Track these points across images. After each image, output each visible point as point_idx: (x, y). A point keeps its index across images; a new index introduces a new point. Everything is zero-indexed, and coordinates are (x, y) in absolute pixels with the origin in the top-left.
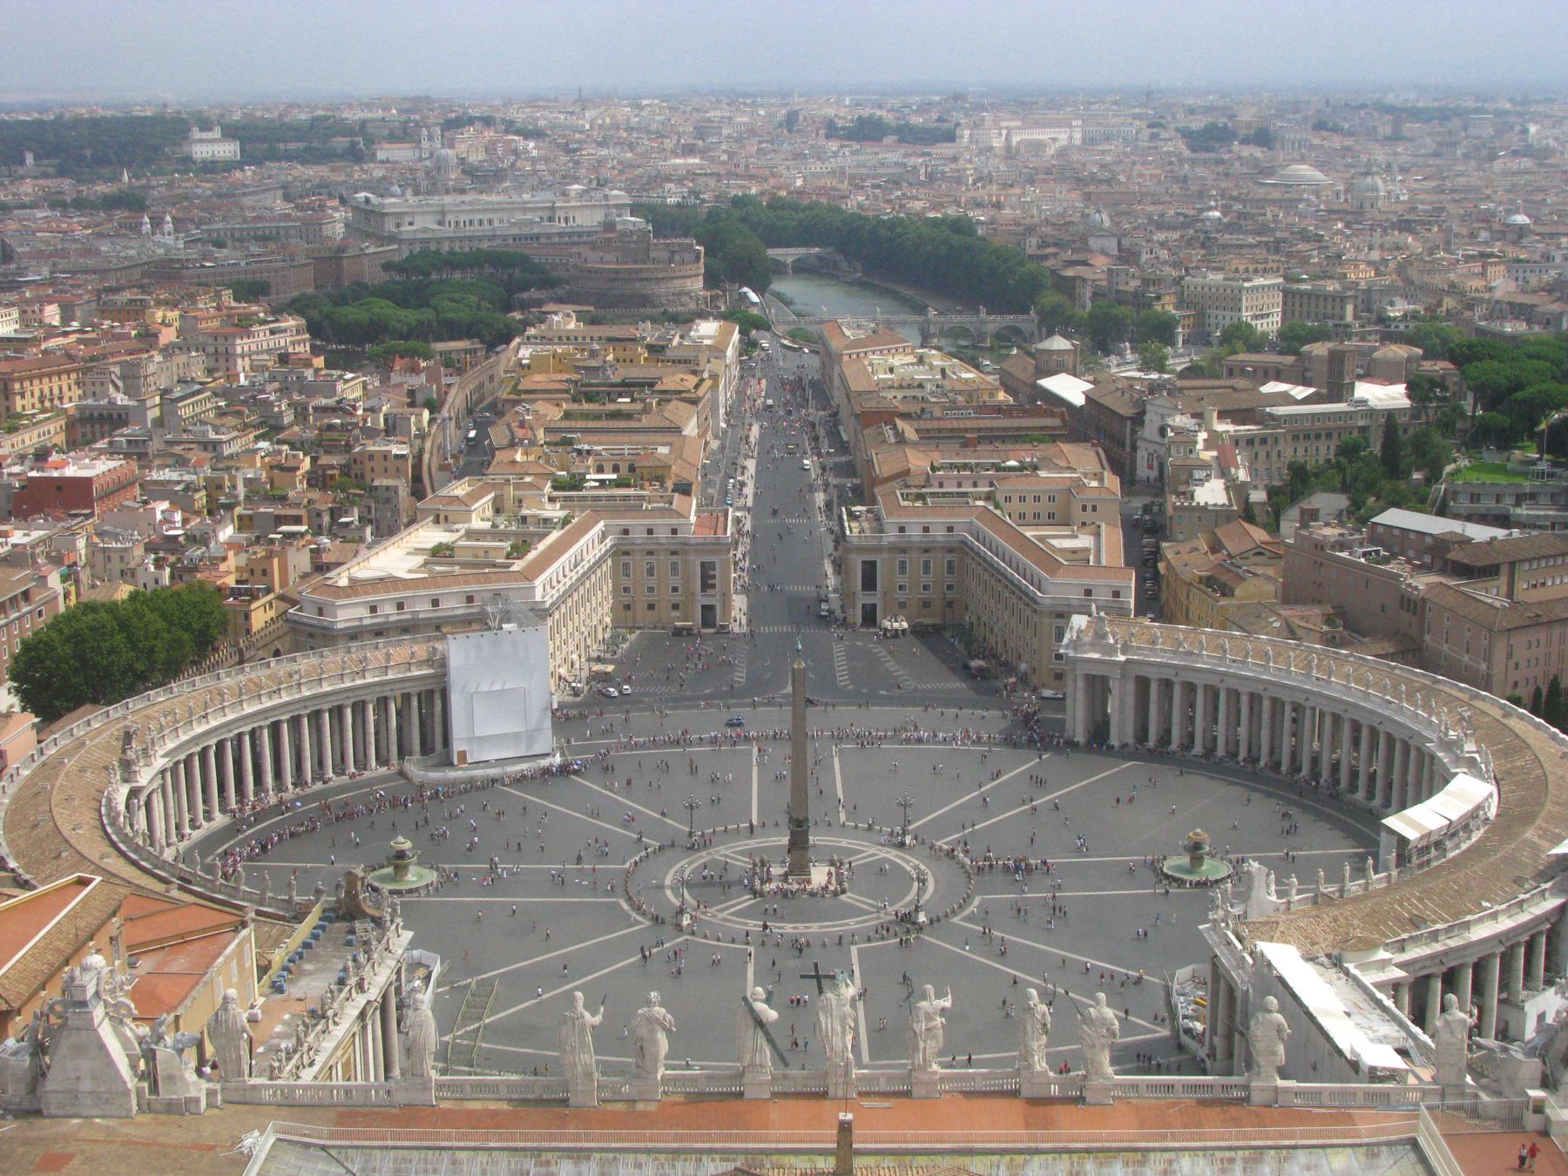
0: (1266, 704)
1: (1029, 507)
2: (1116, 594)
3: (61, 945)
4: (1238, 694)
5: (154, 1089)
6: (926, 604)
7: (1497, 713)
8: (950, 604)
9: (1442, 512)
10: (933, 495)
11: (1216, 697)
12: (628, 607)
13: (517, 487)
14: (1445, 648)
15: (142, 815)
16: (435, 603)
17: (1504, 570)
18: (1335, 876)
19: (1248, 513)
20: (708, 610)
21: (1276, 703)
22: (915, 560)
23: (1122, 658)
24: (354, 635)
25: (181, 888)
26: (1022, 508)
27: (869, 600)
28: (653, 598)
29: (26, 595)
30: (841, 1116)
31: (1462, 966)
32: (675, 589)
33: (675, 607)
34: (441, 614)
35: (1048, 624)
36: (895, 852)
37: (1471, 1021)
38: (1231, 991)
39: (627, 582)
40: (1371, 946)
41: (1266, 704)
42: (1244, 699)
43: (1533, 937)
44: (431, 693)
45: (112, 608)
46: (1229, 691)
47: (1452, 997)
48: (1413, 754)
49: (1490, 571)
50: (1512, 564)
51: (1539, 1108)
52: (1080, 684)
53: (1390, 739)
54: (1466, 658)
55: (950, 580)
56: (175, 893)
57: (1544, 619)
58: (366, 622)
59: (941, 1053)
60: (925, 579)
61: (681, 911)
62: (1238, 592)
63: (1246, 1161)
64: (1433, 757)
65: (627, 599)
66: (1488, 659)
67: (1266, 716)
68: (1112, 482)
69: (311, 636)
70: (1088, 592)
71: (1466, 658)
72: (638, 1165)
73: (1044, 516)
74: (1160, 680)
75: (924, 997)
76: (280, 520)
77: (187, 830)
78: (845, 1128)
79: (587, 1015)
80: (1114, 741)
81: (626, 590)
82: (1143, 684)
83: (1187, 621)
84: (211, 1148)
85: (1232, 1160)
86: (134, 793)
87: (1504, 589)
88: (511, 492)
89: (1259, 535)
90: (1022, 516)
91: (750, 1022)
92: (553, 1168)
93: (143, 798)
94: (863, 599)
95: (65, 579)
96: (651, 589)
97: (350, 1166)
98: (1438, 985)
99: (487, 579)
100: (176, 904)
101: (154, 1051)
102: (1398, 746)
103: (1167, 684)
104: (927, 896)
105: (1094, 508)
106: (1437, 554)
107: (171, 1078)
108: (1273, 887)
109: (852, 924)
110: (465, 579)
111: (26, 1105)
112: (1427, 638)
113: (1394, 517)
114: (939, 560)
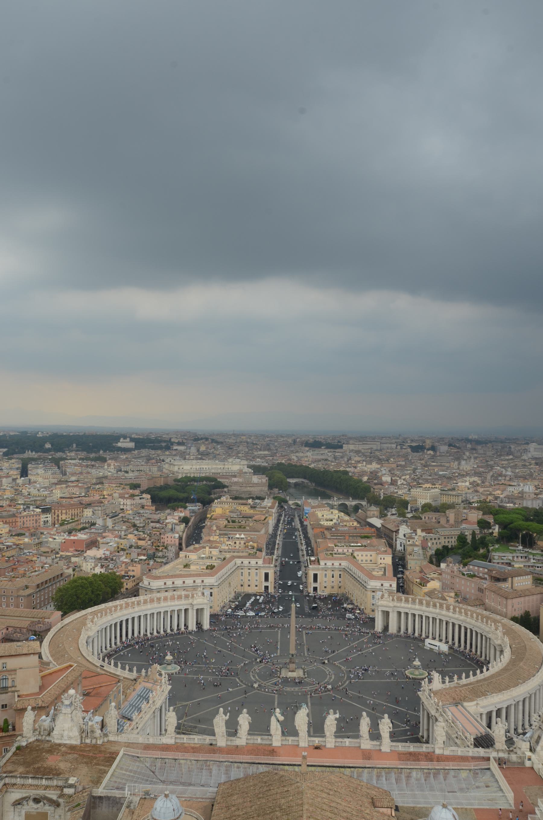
0: (438, 621)
1: (364, 558)
2: (391, 585)
3: (63, 685)
6: (333, 587)
8: (340, 587)
9: (490, 562)
10: (335, 554)
11: (422, 618)
12: (242, 586)
13: (210, 548)
14: (493, 604)
16: (184, 582)
17: (510, 579)
18: (460, 678)
19: (431, 562)
20: (266, 588)
21: (440, 620)
22: (329, 573)
23: (391, 604)
24: (159, 591)
25: (101, 668)
26: (362, 558)
27: (315, 586)
28: (249, 583)
29: (62, 574)
30: (303, 753)
31: (502, 708)
32: (257, 580)
33: (256, 586)
34: (185, 585)
35: (370, 594)
36: (322, 665)
37: (506, 727)
38: (428, 714)
39: (242, 578)
40: (471, 700)
41: (438, 621)
42: (431, 619)
44: (181, 610)
45: (86, 579)
46: (426, 616)
47: (499, 719)
48: (484, 637)
49: (505, 580)
50: (512, 578)
52: (380, 613)
53: (477, 633)
54: (499, 607)
56: (99, 670)
57: (523, 595)
58: (163, 587)
59: (335, 733)
61: (255, 682)
62: (428, 585)
63: (434, 774)
64: (490, 639)
66: (506, 608)
68: (390, 550)
69: (146, 591)
70: (382, 585)
71: (499, 607)
72: (238, 768)
73: (369, 562)
74: (404, 612)
75: (329, 714)
76: (138, 555)
77: (104, 650)
78: (304, 757)
79: (224, 716)
81: (242, 580)
82: (399, 613)
83: (413, 594)
85: (429, 773)
86: (89, 637)
87: (510, 586)
88: (207, 548)
89: (434, 567)
90: (362, 561)
91: (275, 720)
92: (211, 767)
94: (314, 585)
95: (74, 570)
96: (249, 580)
97: (146, 764)
98: (494, 714)
100: (99, 674)
101: (88, 722)
102: (479, 636)
103: (407, 614)
104: (332, 680)
105: (384, 559)
108: (441, 680)
109: (308, 688)
110: (193, 575)
111: (47, 738)
112: (487, 600)
114: (336, 574)
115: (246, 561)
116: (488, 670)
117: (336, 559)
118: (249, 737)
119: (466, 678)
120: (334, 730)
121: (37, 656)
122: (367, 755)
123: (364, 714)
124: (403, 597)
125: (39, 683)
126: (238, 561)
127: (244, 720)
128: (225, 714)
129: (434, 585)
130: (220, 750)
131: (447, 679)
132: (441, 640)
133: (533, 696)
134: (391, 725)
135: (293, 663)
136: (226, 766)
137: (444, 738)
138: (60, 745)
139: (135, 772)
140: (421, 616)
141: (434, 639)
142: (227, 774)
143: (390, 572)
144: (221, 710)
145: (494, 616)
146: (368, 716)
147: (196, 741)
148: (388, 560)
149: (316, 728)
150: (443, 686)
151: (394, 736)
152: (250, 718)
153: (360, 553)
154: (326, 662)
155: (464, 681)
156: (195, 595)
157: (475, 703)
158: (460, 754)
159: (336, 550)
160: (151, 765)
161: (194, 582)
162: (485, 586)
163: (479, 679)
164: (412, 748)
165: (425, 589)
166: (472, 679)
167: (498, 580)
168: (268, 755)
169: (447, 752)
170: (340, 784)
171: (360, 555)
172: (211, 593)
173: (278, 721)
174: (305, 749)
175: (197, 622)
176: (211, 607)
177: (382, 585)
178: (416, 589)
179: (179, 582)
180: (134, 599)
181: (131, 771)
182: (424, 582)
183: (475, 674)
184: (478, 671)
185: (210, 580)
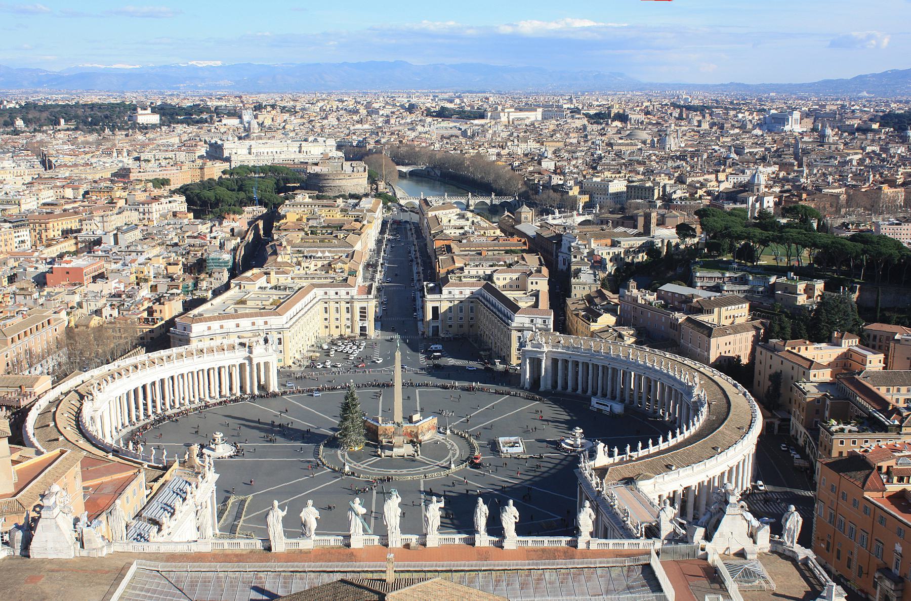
2: (545, 322)
4: (597, 366)
5: (82, 546)
6: (461, 326)
7: (710, 374)
8: (471, 326)
9: (691, 284)
12: (327, 327)
13: (277, 273)
15: (98, 421)
16: (238, 326)
17: (716, 310)
20: (363, 329)
21: (613, 369)
23: (545, 349)
24: (200, 338)
28: (338, 323)
32: (348, 319)
33: (348, 327)
34: (239, 329)
39: (327, 316)
43: (723, 474)
49: (710, 312)
51: (703, 549)
55: (472, 315)
56: (110, 456)
58: (206, 333)
60: (461, 315)
65: (326, 323)
66: (708, 349)
67: (610, 376)
68: (545, 271)
70: (532, 321)
72: (301, 579)
79: (280, 511)
80: (542, 388)
81: (326, 319)
82: (555, 362)
84: (107, 572)
88: (273, 274)
93: (99, 413)
95: (68, 314)
99: (261, 315)
103: (567, 361)
106: (685, 304)
107: (89, 540)
113: (669, 287)
115: (331, 292)
116: (674, 436)
117: (466, 285)
118: (318, 538)
119: (642, 449)
120: (437, 522)
121: (6, 440)
122: (484, 555)
123: (481, 500)
124: (562, 338)
125: (15, 479)
126: (319, 292)
127: (310, 515)
128: (282, 508)
129: (607, 320)
130: (279, 557)
131: (616, 450)
132: (613, 398)
133: (734, 469)
134: (517, 515)
135: (400, 435)
136: (285, 578)
137: (591, 529)
138: (43, 561)
139: (155, 591)
140: (587, 365)
141: (604, 395)
142: (285, 587)
143: (544, 302)
144: (276, 503)
145: (688, 361)
146: (485, 503)
147: (242, 547)
148: (542, 285)
149: (412, 521)
150: (611, 460)
151: (521, 530)
152: (317, 512)
153: (501, 276)
154: (448, 432)
155: (642, 453)
156: (254, 344)
157: (652, 480)
158: (611, 547)
159: (466, 272)
160: (177, 581)
161: (253, 324)
162: (680, 321)
163: (661, 448)
164: (546, 541)
165: (594, 327)
166: (652, 449)
167: (700, 311)
168: (343, 561)
169: (593, 546)
170: (439, 593)
171: (501, 279)
172: (280, 339)
173: (357, 515)
174: (392, 551)
175: (259, 381)
176: (280, 361)
177: (532, 321)
178: (580, 324)
179: (230, 324)
180: (163, 353)
181: (148, 591)
182: (592, 315)
183: (655, 443)
184: (661, 439)
185: (275, 321)
